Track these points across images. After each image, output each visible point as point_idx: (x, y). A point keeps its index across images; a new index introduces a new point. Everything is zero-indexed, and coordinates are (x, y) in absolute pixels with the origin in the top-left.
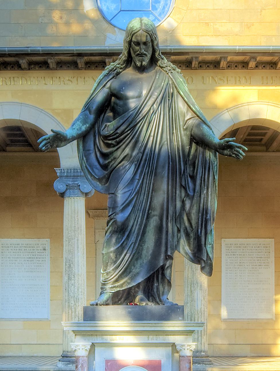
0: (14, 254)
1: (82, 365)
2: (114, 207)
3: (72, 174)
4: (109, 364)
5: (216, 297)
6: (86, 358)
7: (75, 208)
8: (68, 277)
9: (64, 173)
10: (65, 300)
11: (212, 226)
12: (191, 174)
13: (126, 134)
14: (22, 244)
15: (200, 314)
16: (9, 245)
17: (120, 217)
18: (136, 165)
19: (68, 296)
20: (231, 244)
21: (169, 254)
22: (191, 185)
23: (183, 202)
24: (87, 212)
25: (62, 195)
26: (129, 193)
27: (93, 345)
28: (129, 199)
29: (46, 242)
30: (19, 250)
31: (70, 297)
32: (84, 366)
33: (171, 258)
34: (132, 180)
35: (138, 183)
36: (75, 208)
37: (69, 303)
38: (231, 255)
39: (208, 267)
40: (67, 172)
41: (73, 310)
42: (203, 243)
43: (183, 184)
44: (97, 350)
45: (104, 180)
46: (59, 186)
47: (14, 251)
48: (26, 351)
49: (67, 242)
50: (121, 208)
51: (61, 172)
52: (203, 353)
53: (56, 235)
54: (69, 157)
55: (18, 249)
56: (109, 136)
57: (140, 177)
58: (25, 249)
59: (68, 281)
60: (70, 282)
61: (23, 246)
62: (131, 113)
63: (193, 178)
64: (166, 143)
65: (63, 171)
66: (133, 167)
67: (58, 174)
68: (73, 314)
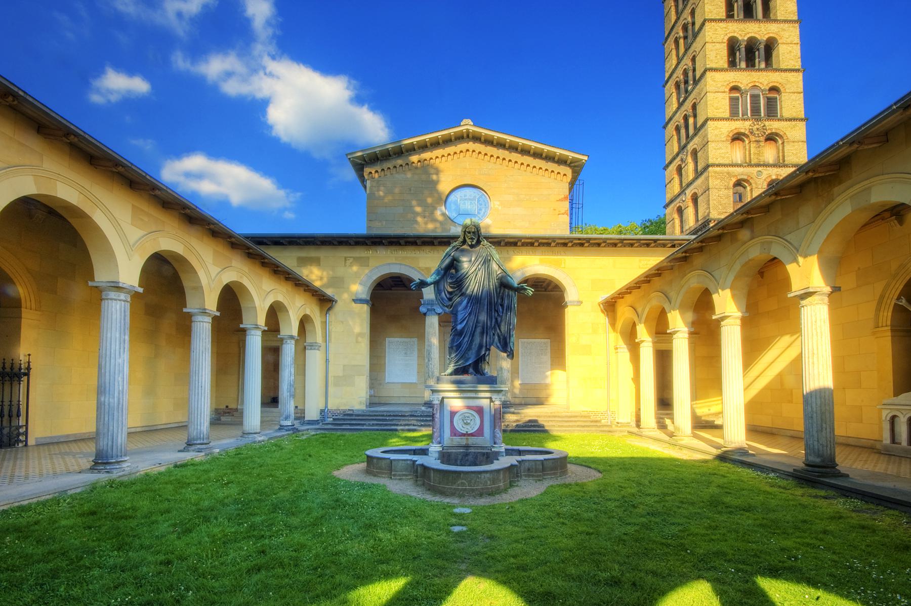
2: (455, 321)
3: (430, 303)
5: (515, 372)
7: (432, 322)
11: (514, 333)
17: (459, 327)
24: (440, 324)
25: (425, 314)
29: (415, 340)
33: (489, 350)
36: (432, 322)
39: (511, 355)
46: (423, 309)
48: (402, 401)
53: (421, 336)
54: (429, 293)
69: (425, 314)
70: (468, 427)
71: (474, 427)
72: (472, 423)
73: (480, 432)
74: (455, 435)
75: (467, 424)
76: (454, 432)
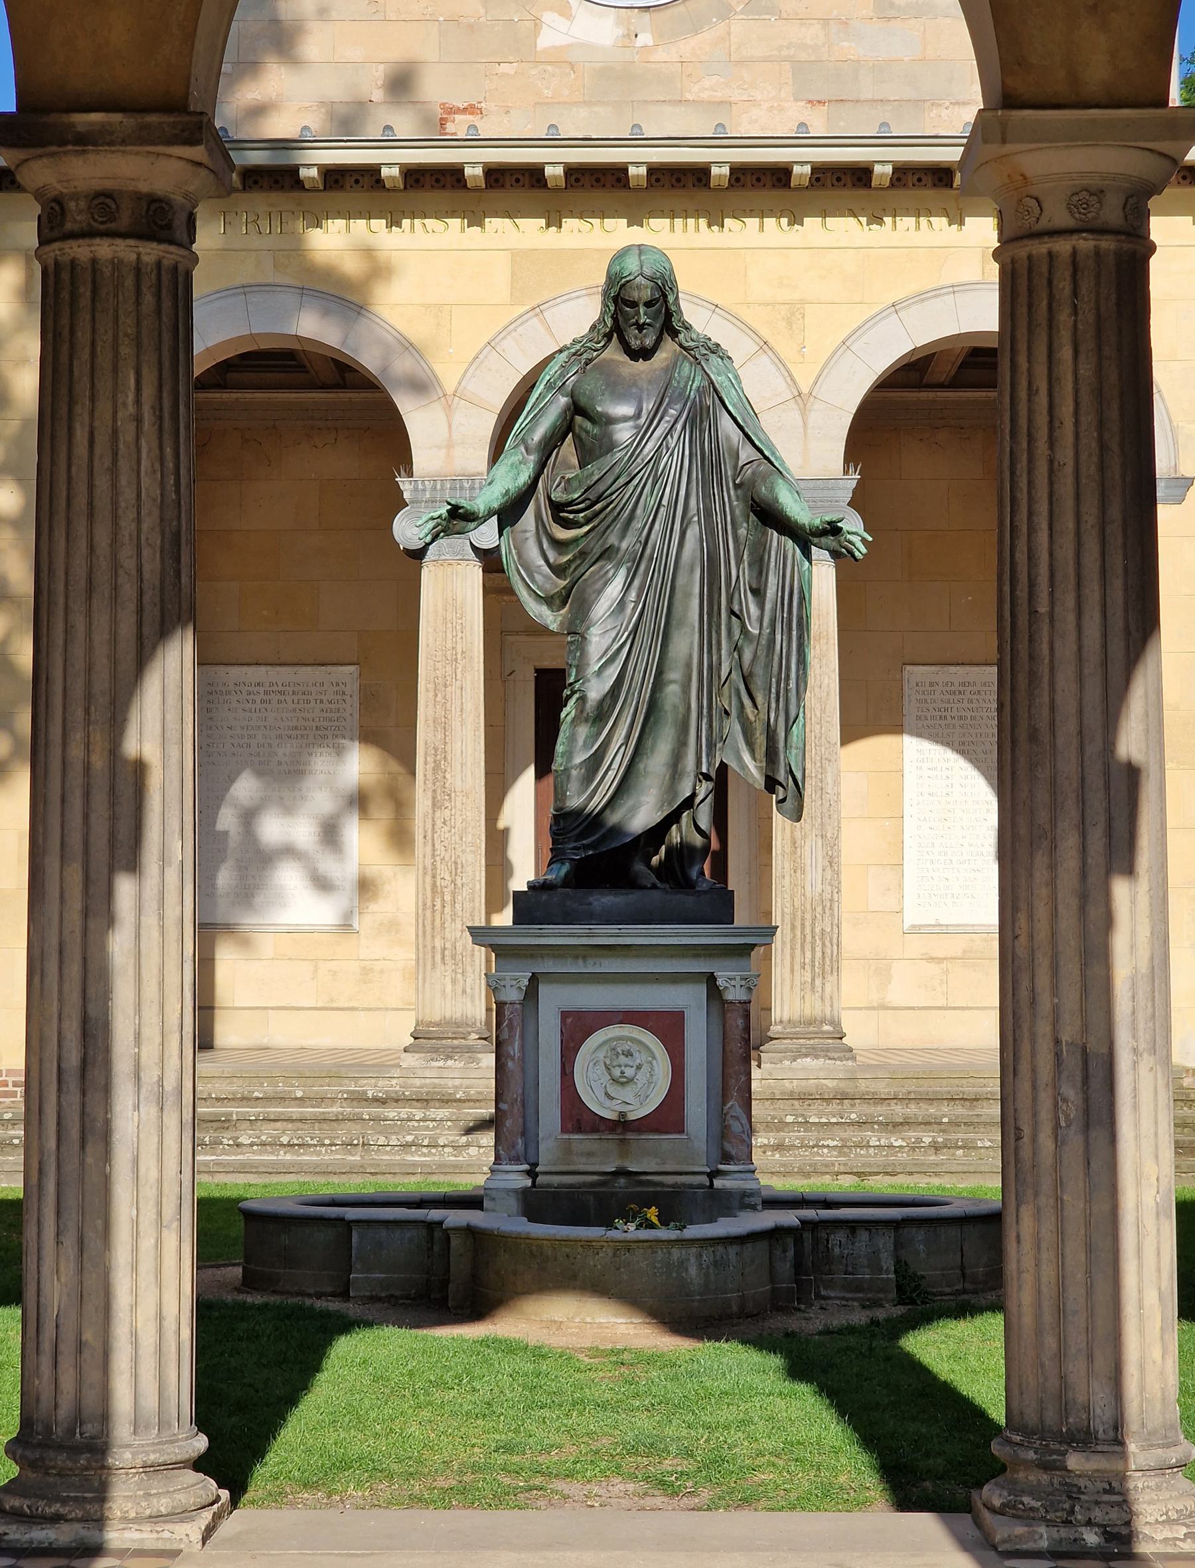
0: (247, 714)
1: (510, 1020)
4: (569, 1020)
6: (518, 1006)
8: (434, 798)
9: (424, 490)
10: (425, 868)
12: (754, 586)
13: (609, 500)
14: (271, 684)
15: (819, 909)
16: (232, 687)
18: (629, 570)
19: (433, 856)
20: (931, 684)
21: (704, 770)
22: (754, 610)
23: (737, 648)
25: (418, 555)
26: (613, 634)
27: (534, 979)
28: (616, 646)
30: (263, 701)
31: (438, 859)
32: (515, 1024)
34: (622, 604)
35: (635, 609)
37: (434, 876)
38: (933, 718)
40: (434, 489)
41: (448, 898)
42: (781, 745)
43: (736, 608)
44: (544, 990)
45: (558, 602)
46: (408, 529)
47: (248, 706)
49: (431, 694)
50: (596, 668)
51: (416, 489)
52: (826, 1028)
55: (258, 698)
56: (571, 503)
57: (639, 596)
58: (282, 698)
59: (430, 811)
60: (438, 814)
61: (275, 688)
62: (619, 455)
63: (758, 593)
64: (696, 519)
65: (420, 487)
66: (623, 572)
67: (406, 496)
68: (447, 910)
69: (418, 555)
70: (627, 1094)
71: (644, 1099)
72: (641, 1077)
73: (668, 1117)
74: (579, 1129)
75: (623, 1082)
76: (577, 1117)
